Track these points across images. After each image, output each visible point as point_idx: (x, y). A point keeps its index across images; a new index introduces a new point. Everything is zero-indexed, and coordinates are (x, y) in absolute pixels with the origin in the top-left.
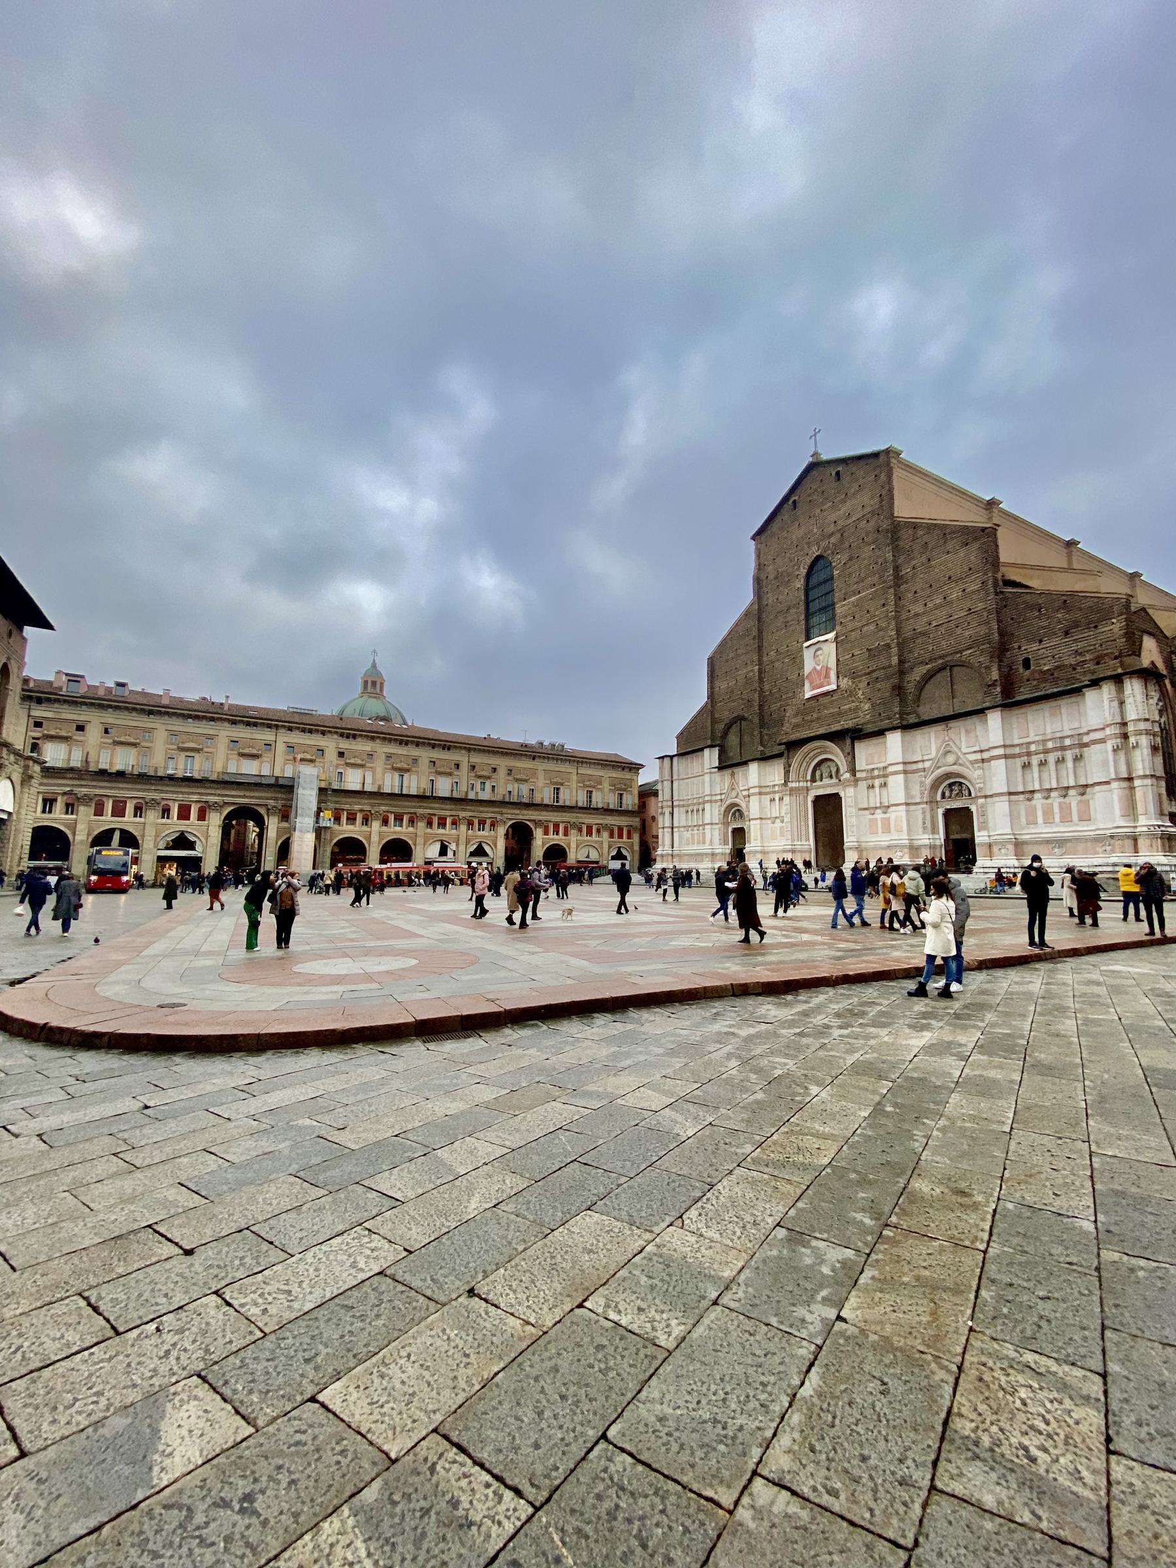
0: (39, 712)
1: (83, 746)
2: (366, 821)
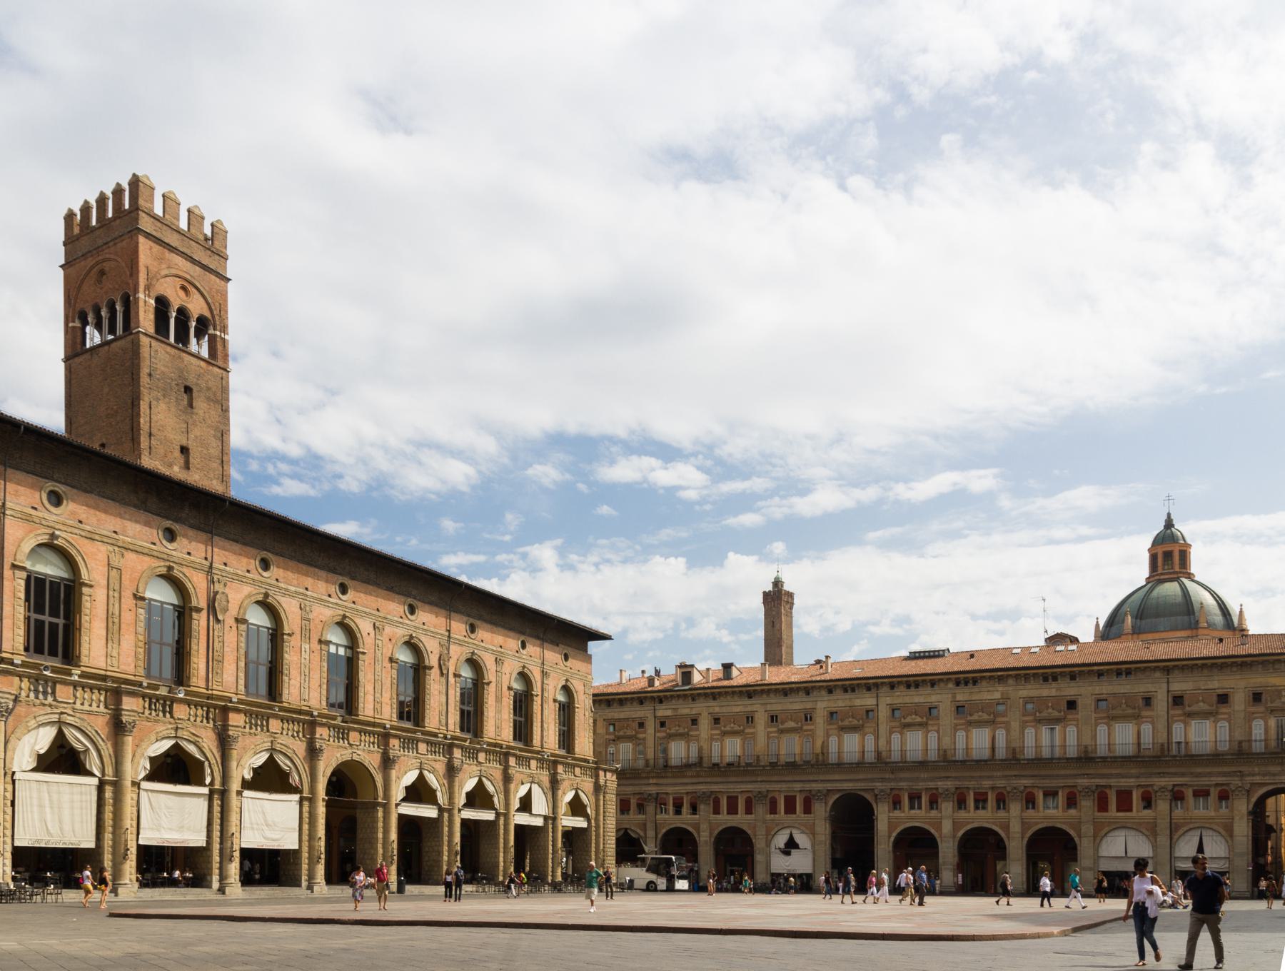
0: (664, 711)
1: (698, 740)
2: (1001, 801)
